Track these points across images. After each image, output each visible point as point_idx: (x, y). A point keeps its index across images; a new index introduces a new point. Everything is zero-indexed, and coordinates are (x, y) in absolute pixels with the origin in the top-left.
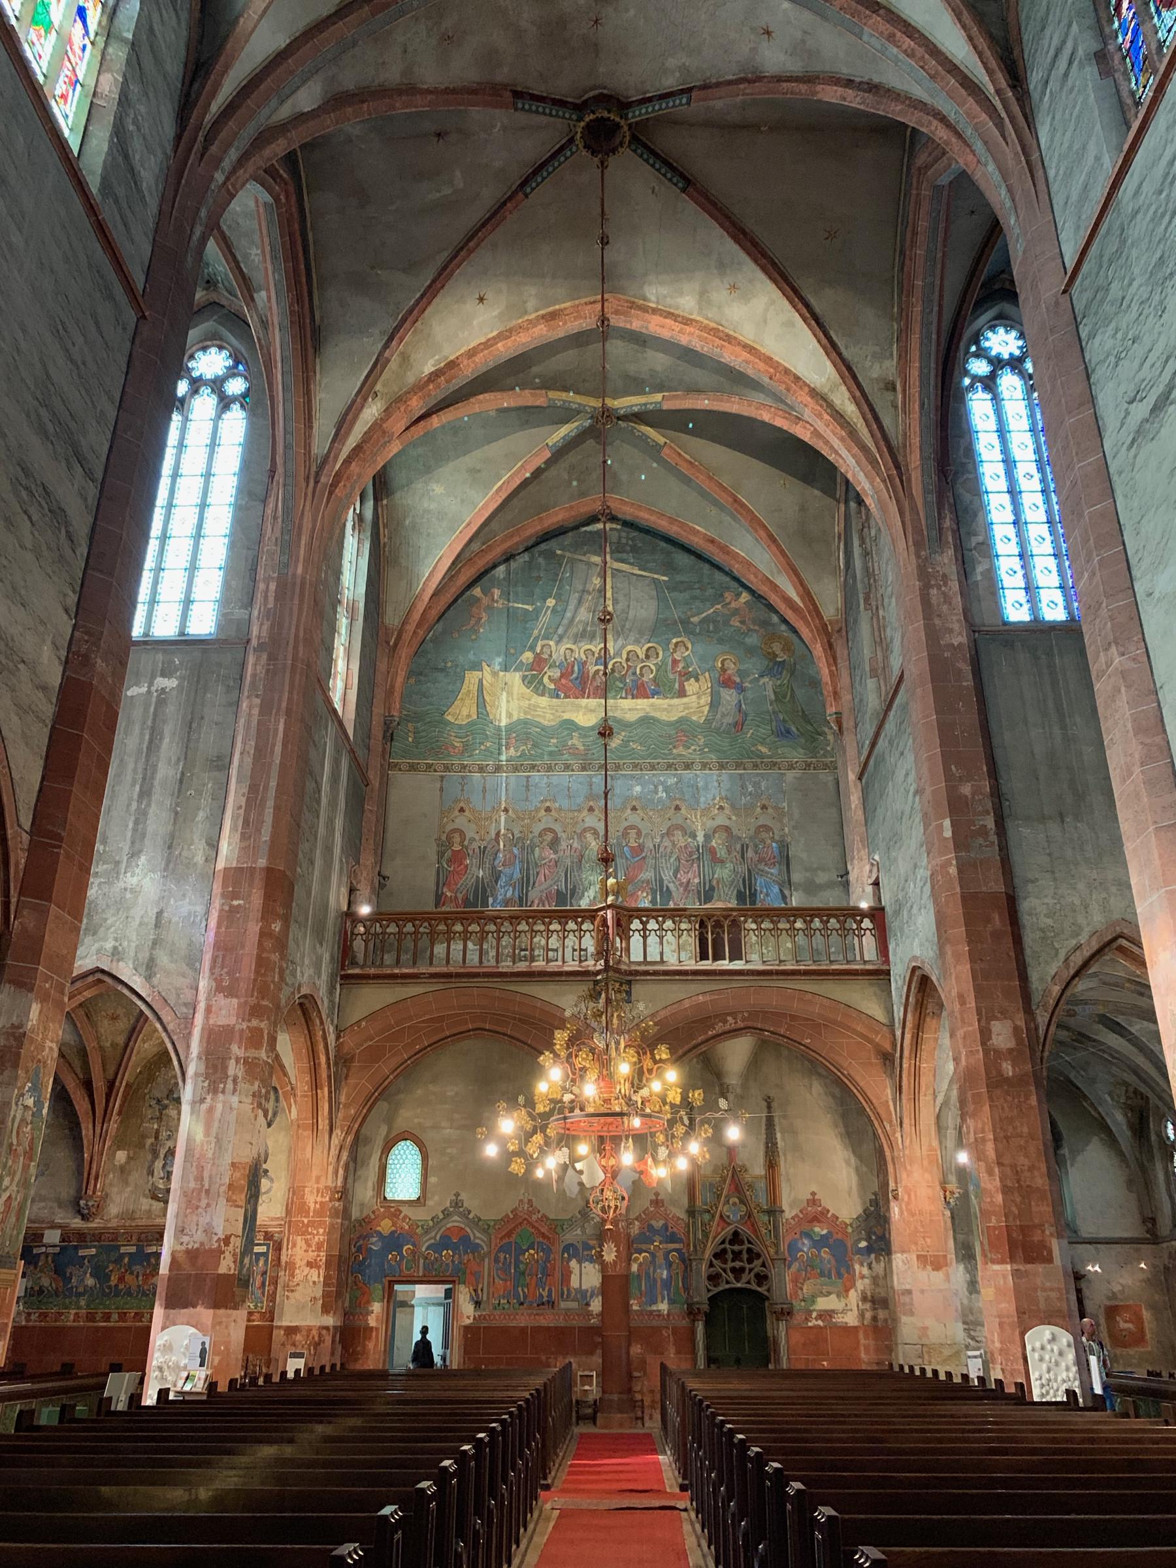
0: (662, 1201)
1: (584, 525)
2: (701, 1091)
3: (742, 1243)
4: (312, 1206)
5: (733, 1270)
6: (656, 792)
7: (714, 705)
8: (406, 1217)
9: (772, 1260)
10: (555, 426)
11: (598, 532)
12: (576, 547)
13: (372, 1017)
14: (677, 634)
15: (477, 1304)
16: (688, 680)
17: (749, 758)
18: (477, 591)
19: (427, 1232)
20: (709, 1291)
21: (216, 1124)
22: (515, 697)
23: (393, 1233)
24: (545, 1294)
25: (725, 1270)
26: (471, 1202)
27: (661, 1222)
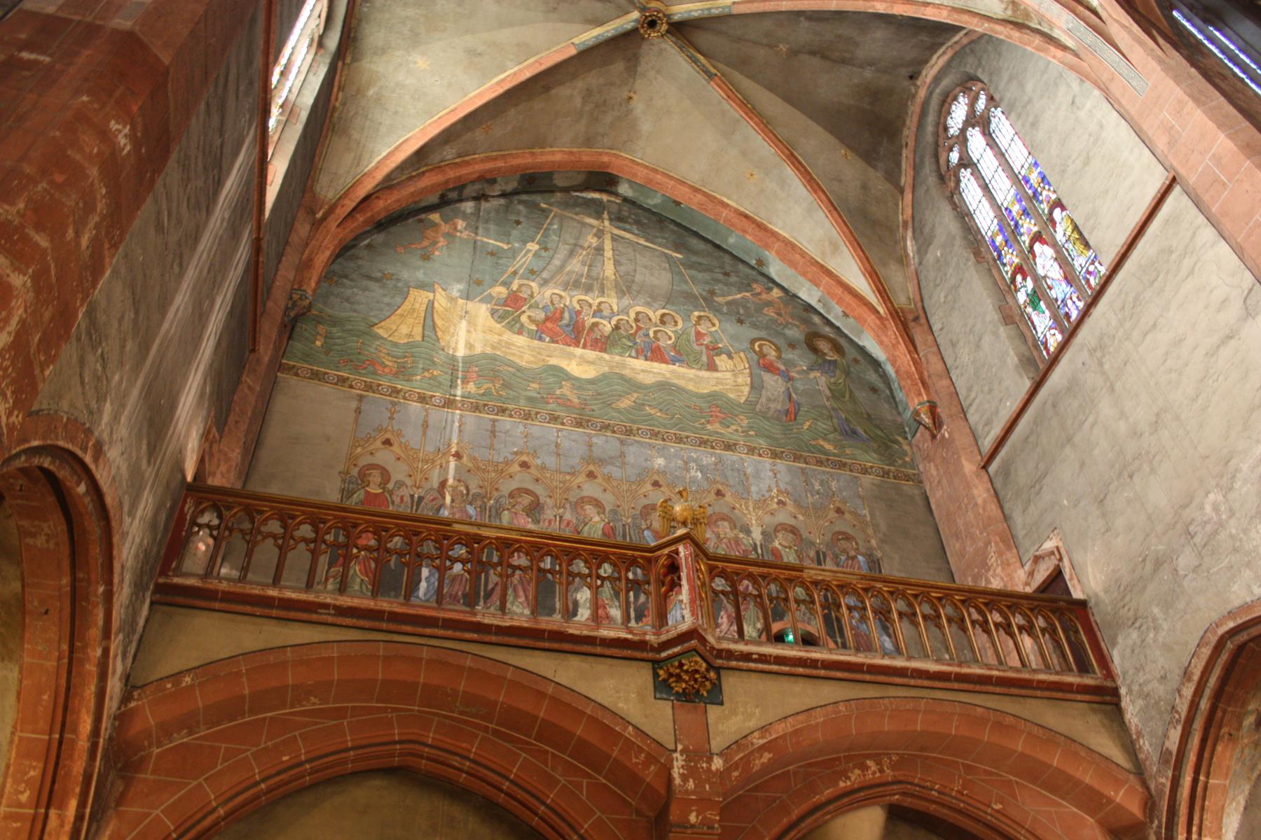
1: (576, 191)
6: (688, 470)
7: (757, 387)
10: (587, 26)
11: (593, 201)
12: (566, 205)
13: (209, 671)
14: (697, 308)
16: (718, 355)
17: (810, 451)
18: (435, 217)
22: (479, 328)
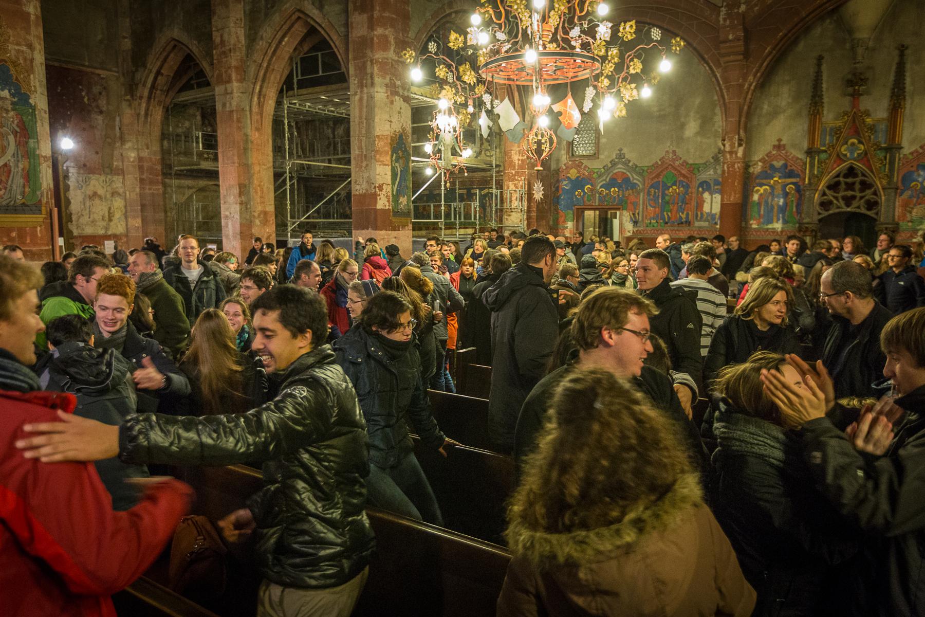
0: (784, 146)
2: (633, 23)
3: (856, 175)
4: (517, 162)
5: (844, 198)
8: (586, 166)
9: (884, 189)
15: (635, 223)
19: (600, 176)
20: (819, 214)
21: (365, 110)
23: (578, 177)
24: (684, 216)
25: (836, 198)
26: (630, 154)
27: (782, 162)
